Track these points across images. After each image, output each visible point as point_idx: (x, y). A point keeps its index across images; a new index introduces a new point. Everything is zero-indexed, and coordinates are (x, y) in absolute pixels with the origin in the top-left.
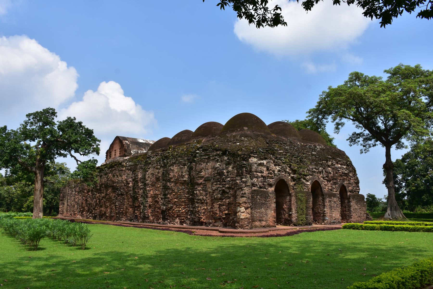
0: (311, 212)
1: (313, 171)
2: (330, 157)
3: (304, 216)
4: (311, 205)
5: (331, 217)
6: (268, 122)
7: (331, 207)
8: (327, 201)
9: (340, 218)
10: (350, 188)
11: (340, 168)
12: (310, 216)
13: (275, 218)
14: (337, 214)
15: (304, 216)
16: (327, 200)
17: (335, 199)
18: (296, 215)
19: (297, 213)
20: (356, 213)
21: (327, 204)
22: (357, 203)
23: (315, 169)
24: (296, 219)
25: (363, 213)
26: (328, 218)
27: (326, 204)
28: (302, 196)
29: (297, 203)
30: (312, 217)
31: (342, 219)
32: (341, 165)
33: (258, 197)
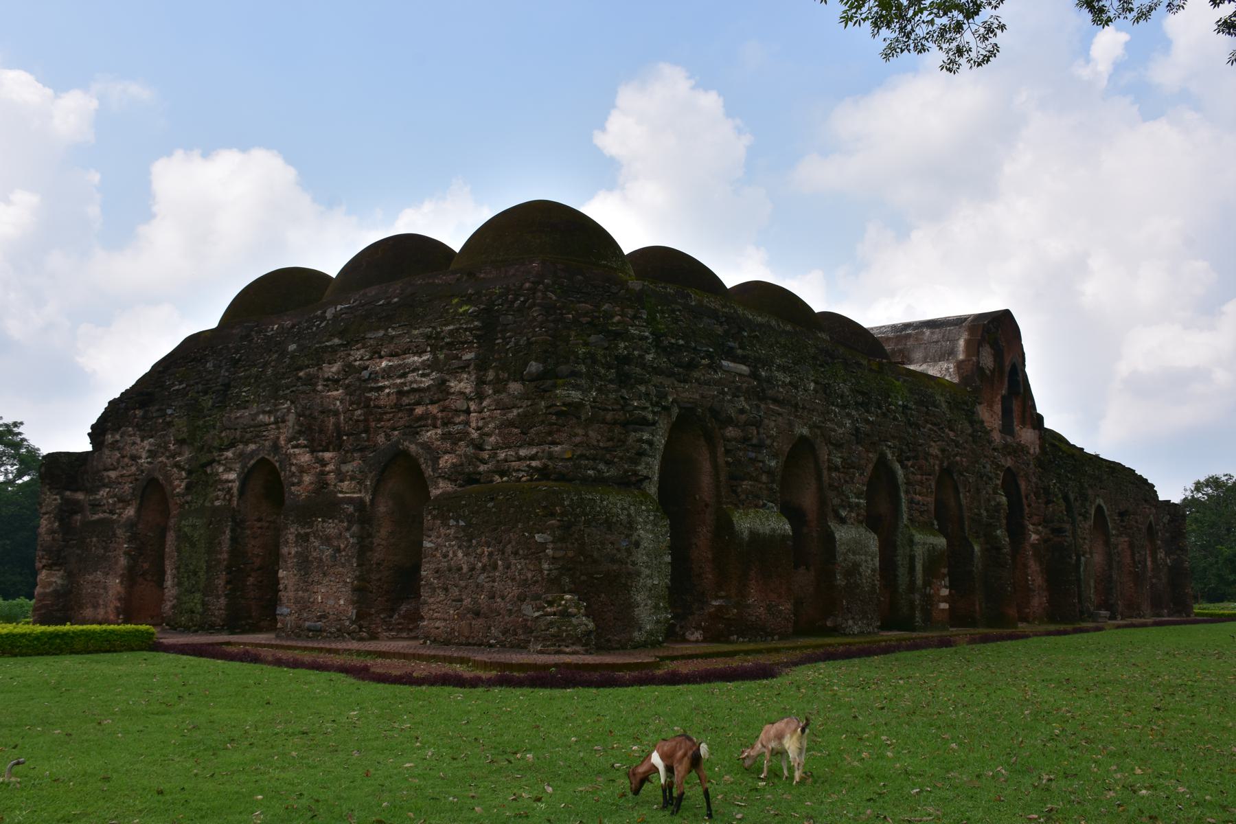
0: (221, 582)
1: (255, 426)
2: (336, 341)
3: (198, 595)
4: (225, 556)
5: (304, 605)
6: (332, 269)
7: (304, 564)
8: (291, 538)
9: (352, 612)
10: (446, 461)
11: (388, 373)
12: (218, 597)
13: (119, 600)
14: (333, 596)
15: (198, 595)
16: (292, 532)
17: (331, 528)
18: (174, 591)
19: (179, 584)
20: (455, 592)
21: (290, 550)
22: (467, 538)
23: (264, 412)
24: (174, 607)
25: (513, 591)
26: (285, 610)
27: (285, 550)
28: (194, 526)
29: (178, 550)
30: (223, 601)
31: (360, 616)
32: (392, 355)
33: (94, 539)
